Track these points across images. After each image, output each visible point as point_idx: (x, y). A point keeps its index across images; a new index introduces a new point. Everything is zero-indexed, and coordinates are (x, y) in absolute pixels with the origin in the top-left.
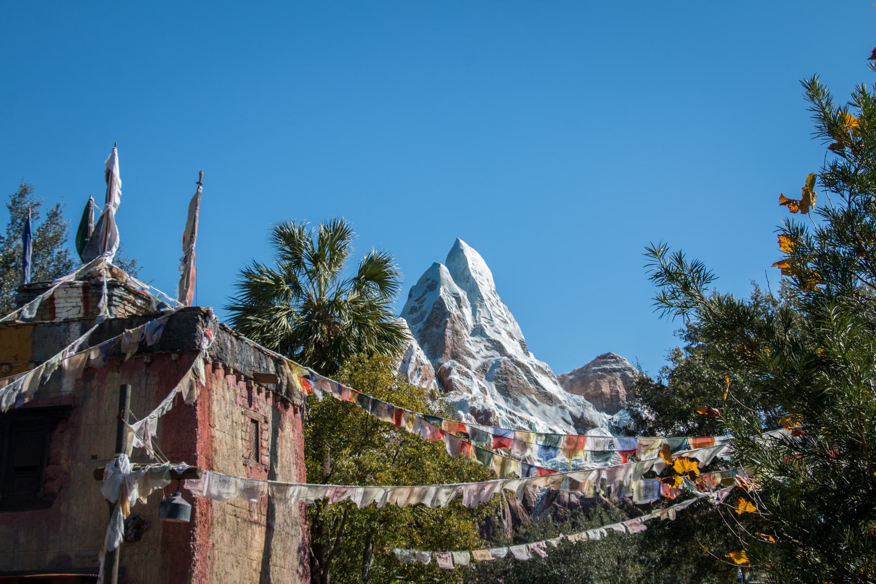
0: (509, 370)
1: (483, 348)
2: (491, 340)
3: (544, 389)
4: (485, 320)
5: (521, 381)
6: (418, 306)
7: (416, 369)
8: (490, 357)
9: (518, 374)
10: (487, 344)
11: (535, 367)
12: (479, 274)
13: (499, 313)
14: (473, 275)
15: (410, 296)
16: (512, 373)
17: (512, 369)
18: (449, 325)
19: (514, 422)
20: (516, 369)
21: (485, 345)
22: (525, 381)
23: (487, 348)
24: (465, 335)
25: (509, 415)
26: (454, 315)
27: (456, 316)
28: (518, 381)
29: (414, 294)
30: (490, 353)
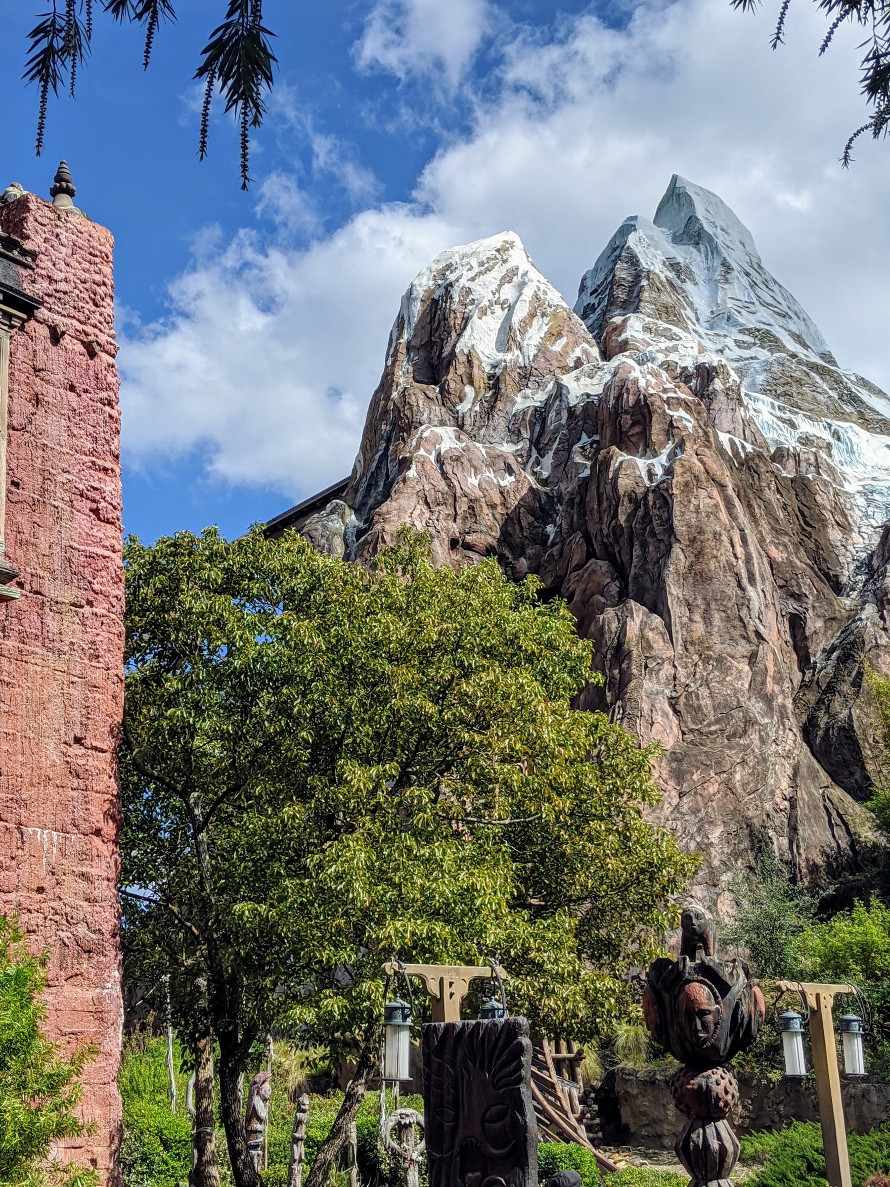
0: (792, 377)
1: (732, 344)
2: (747, 330)
3: (878, 413)
4: (736, 303)
5: (821, 398)
6: (596, 301)
7: (532, 315)
8: (747, 359)
9: (814, 385)
10: (741, 337)
11: (853, 378)
12: (722, 229)
13: (770, 300)
14: (707, 227)
15: (583, 288)
16: (799, 382)
17: (798, 374)
18: (646, 295)
19: (792, 425)
20: (808, 374)
21: (735, 341)
22: (830, 397)
23: (739, 344)
24: (689, 318)
25: (778, 413)
26: (659, 277)
27: (664, 280)
28: (814, 398)
29: (589, 283)
30: (746, 353)
